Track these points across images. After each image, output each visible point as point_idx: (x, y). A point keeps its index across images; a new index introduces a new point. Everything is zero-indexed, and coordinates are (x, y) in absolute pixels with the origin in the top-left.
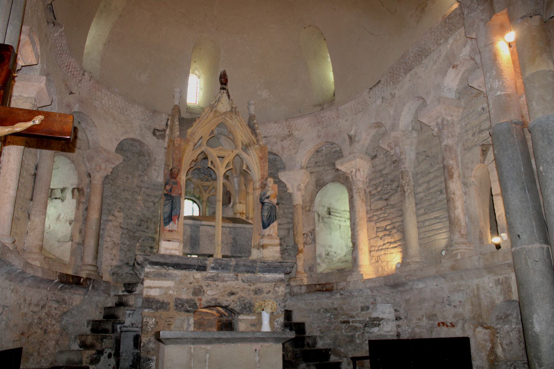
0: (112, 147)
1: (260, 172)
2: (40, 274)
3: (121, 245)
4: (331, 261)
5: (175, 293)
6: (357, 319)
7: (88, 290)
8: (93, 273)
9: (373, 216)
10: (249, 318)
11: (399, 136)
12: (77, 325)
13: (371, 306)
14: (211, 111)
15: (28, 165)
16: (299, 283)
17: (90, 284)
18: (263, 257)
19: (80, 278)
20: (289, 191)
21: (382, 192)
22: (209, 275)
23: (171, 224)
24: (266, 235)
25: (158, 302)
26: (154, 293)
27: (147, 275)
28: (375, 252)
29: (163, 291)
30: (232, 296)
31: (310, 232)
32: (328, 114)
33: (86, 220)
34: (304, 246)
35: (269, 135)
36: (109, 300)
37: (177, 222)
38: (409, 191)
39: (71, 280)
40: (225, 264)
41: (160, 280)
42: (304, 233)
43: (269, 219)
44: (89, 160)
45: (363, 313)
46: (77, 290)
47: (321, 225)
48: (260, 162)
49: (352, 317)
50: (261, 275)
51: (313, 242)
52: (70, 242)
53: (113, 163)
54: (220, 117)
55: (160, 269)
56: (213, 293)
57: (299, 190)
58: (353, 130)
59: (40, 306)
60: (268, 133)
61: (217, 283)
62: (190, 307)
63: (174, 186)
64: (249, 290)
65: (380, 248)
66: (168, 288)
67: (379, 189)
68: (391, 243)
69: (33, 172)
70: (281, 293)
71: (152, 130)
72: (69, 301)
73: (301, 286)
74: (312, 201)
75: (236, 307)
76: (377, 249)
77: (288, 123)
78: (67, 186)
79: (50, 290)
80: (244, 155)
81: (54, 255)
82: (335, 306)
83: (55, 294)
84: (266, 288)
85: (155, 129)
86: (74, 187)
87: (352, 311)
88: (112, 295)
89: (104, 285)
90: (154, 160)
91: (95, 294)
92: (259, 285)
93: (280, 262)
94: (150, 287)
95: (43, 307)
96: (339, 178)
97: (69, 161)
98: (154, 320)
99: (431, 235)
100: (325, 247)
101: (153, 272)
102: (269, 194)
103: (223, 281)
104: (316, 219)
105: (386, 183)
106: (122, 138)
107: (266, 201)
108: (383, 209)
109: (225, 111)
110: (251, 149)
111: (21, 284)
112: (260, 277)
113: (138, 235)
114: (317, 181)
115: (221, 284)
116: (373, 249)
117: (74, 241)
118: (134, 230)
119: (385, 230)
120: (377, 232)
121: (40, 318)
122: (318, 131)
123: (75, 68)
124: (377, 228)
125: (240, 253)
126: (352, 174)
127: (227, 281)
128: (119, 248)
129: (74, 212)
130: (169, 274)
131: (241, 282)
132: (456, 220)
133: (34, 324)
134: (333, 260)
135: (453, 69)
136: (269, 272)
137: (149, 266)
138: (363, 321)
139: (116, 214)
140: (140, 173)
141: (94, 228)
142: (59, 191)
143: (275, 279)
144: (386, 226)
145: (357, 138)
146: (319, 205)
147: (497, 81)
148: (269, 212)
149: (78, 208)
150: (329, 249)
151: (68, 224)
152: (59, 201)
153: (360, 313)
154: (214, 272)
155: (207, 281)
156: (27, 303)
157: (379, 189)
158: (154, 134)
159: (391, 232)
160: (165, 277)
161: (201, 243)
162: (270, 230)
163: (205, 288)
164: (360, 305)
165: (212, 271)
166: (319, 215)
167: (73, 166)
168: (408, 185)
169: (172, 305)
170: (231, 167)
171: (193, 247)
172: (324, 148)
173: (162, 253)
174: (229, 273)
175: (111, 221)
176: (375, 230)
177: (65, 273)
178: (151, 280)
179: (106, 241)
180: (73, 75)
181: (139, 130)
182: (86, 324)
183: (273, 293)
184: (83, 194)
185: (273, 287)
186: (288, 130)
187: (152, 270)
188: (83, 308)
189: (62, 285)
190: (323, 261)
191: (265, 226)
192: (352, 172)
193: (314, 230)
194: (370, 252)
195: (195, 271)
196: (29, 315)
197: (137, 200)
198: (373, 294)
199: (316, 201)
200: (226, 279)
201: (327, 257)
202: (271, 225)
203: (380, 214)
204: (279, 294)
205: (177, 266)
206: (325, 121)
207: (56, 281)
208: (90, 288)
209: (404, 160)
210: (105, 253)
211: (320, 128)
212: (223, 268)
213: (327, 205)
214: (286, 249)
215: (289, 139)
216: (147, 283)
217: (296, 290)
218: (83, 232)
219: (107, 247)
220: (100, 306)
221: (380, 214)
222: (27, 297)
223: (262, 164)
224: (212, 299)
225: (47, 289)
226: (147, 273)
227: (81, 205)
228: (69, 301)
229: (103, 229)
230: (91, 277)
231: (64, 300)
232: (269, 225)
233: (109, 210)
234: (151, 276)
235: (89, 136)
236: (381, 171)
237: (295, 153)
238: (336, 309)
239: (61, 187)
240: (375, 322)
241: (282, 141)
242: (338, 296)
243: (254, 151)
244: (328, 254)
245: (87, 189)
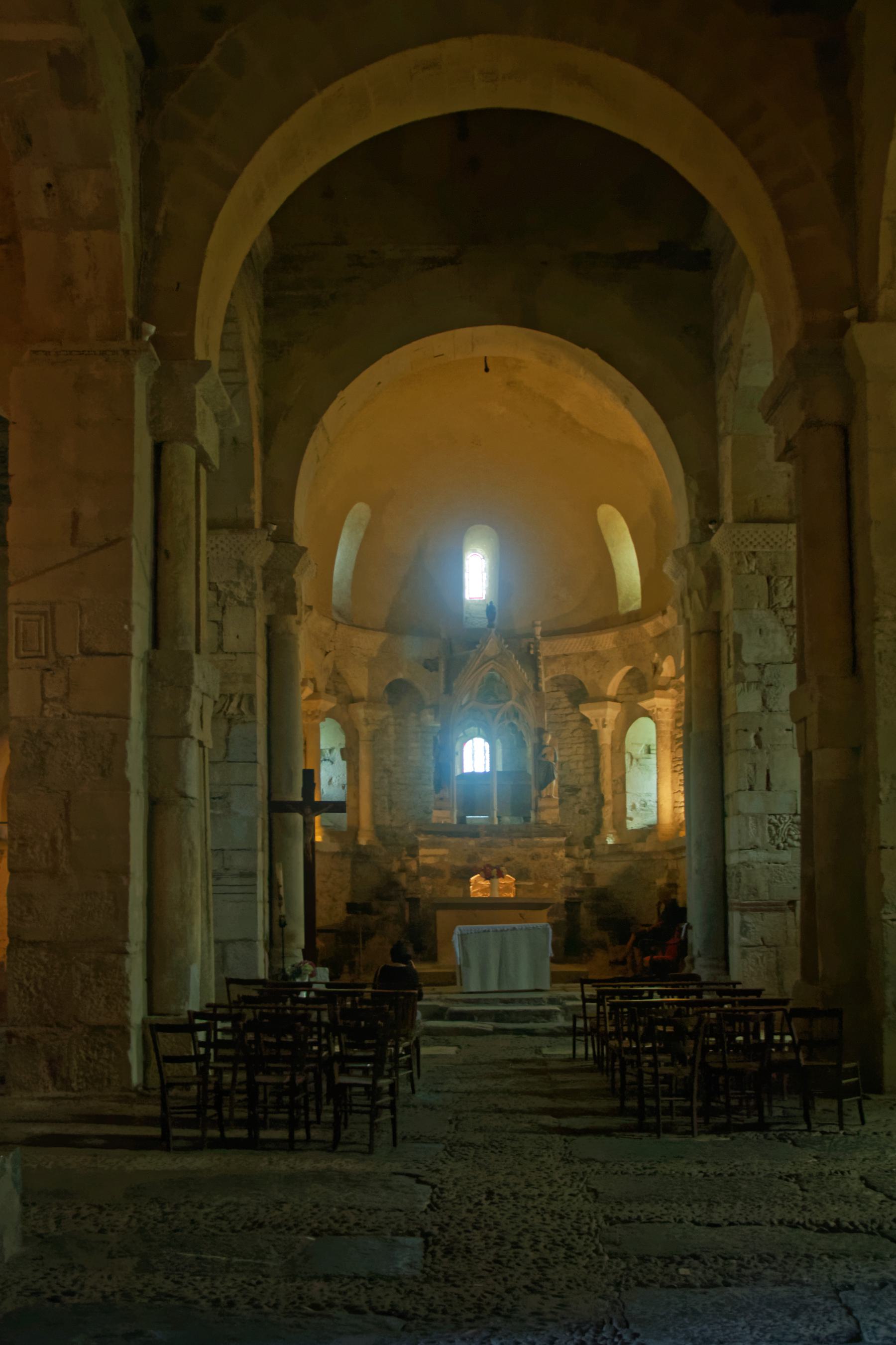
22: (483, 841)
26: (430, 861)
60: (568, 649)
66: (444, 856)
77: (589, 638)
86: (343, 746)
104: (628, 762)
106: (388, 682)
136: (547, 836)
142: (328, 751)
150: (647, 799)
151: (341, 788)
152: (329, 763)
154: (488, 839)
158: (426, 667)
166: (632, 758)
187: (426, 839)
192: (653, 711)
205: (450, 834)
216: (422, 851)
239: (329, 747)
244: (645, 805)
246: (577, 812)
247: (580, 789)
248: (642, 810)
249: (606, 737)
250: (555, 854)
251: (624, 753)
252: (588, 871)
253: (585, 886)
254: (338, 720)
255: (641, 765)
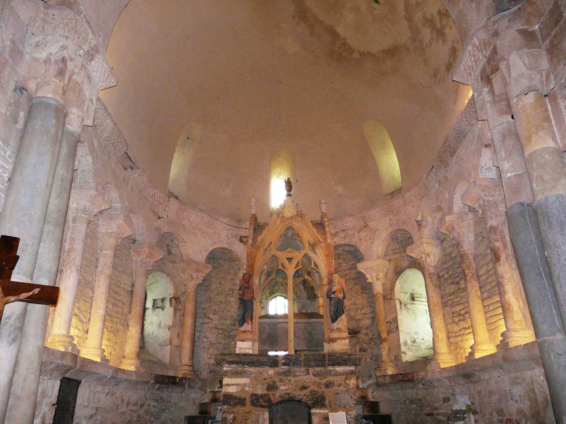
0: (201, 257)
1: (327, 269)
2: (134, 378)
3: (218, 344)
4: (418, 348)
5: (251, 389)
6: (441, 411)
7: (184, 388)
8: (189, 372)
9: (448, 300)
10: (322, 411)
11: (454, 219)
12: (175, 421)
13: (451, 398)
14: (278, 218)
15: (125, 284)
16: (384, 373)
17: (186, 383)
18: (333, 350)
19: (176, 378)
20: (368, 281)
21: (453, 275)
23: (245, 325)
24: (335, 329)
25: (235, 398)
26: (232, 390)
27: (226, 374)
28: (453, 338)
29: (240, 388)
30: (304, 391)
31: (393, 320)
32: (397, 202)
33: (182, 324)
34: (388, 335)
35: (347, 228)
36: (206, 396)
37: (250, 323)
38: (470, 275)
39: (167, 380)
40: (295, 360)
41: (237, 378)
42: (387, 321)
43: (336, 313)
44: (183, 272)
45: (446, 404)
46: (174, 388)
47: (405, 312)
48: (326, 259)
49: (436, 409)
50: (332, 368)
51: (397, 331)
52: (170, 346)
53: (203, 272)
54: (287, 222)
55: (237, 368)
56: (286, 388)
57: (378, 279)
58: (420, 215)
59: (139, 406)
60: (346, 226)
61: (289, 378)
62: (265, 403)
63: (246, 290)
64: (320, 384)
65: (457, 334)
66: (245, 385)
67: (450, 273)
68: (465, 329)
69: (130, 289)
70: (352, 385)
71: (239, 238)
72: (167, 399)
73: (385, 376)
74: (392, 288)
75: (308, 401)
76: (454, 335)
78: (165, 296)
79: (148, 390)
80: (312, 255)
81: (157, 358)
82: (420, 397)
83: (152, 393)
84: (337, 381)
85: (241, 237)
87: (436, 402)
88: (208, 392)
89: (200, 383)
90: (242, 264)
91: (191, 391)
92: (330, 379)
93: (349, 355)
94: (229, 385)
95: (142, 406)
96: (415, 263)
97: (165, 275)
98: (232, 415)
99: (496, 320)
100: (410, 334)
101: (230, 370)
102: (334, 289)
103: (295, 376)
105: (455, 266)
106: (211, 249)
107: (333, 296)
108: (455, 293)
109: (291, 215)
110: (318, 248)
111: (116, 387)
112: (330, 371)
113: (233, 333)
114: (395, 268)
115: (293, 379)
116: (451, 335)
117: (173, 344)
118: (229, 330)
119: (460, 315)
120: (453, 317)
121: (139, 416)
122: (390, 219)
123: (160, 197)
124: (453, 313)
125: (316, 346)
126: (423, 259)
127: (299, 376)
128: (215, 347)
129: (172, 319)
130: (245, 372)
131: (313, 376)
132: (507, 305)
133: (133, 421)
134: (420, 347)
135: (487, 148)
136: (339, 364)
137: (226, 365)
138: (446, 414)
139: (212, 316)
140: (233, 277)
141: (189, 331)
142: (160, 300)
143: (346, 372)
144: (460, 310)
145: (424, 223)
146: (401, 292)
147: (506, 162)
148: (335, 306)
149: (175, 315)
150: (415, 337)
151: (167, 329)
152: (160, 309)
153: (443, 405)
155: (281, 377)
156: (125, 403)
157: (450, 273)
158: (241, 240)
159: (465, 317)
160: (241, 374)
161: (279, 340)
162: (338, 324)
163: (278, 383)
164: (441, 396)
165: (284, 367)
166: (401, 303)
167: (169, 278)
168: (469, 269)
169: (248, 401)
170: (300, 267)
171: (272, 344)
172: (399, 235)
173: (237, 352)
174: (301, 368)
175: (206, 323)
176: (451, 315)
177: (160, 374)
178: (229, 378)
179: (203, 342)
180: (159, 202)
181: (226, 239)
182: (184, 420)
183: (344, 385)
184: (180, 302)
185: (344, 380)
186: (363, 222)
187: (230, 369)
188: (181, 404)
189: (158, 385)
190: (409, 349)
191: (334, 320)
192: (422, 258)
193: (396, 317)
194: (449, 338)
195: (268, 368)
196: (127, 414)
197: (230, 302)
198: (451, 384)
199: (396, 289)
200: (298, 374)
201: (413, 344)
202: (339, 319)
203: (454, 299)
204: (351, 387)
205: (252, 364)
206: (395, 209)
207: (152, 382)
208: (187, 386)
209: (462, 244)
210: (203, 353)
211: (391, 217)
212: (294, 364)
213: (410, 291)
214: (372, 338)
215: (365, 230)
216: (226, 381)
217: (381, 380)
218: (181, 336)
219: (204, 348)
220: (197, 402)
221: (454, 299)
222: (124, 398)
223: (329, 261)
224: (285, 394)
225: (144, 389)
226: (226, 372)
227: (178, 312)
228: (167, 399)
229: (200, 331)
230: (187, 376)
231: (162, 398)
232: (336, 319)
233: (204, 314)
234: (229, 374)
235: (182, 250)
236: (450, 254)
237: (372, 243)
238: (420, 400)
239: (161, 297)
240: (458, 415)
241: (359, 232)
242: (420, 386)
243: (320, 250)
244: (414, 342)
245: (183, 297)
246: (358, 350)
247: (359, 332)
248: (413, 345)
249: (378, 288)
250: (348, 382)
251: (395, 299)
252: (372, 400)
253: (372, 414)
254: (168, 275)
255: (408, 309)
